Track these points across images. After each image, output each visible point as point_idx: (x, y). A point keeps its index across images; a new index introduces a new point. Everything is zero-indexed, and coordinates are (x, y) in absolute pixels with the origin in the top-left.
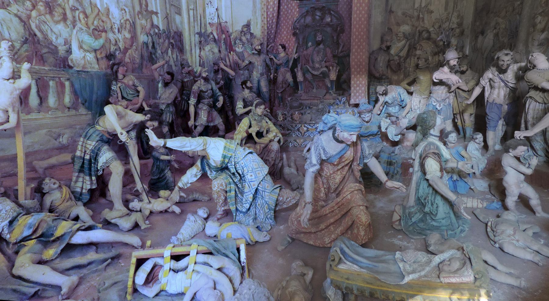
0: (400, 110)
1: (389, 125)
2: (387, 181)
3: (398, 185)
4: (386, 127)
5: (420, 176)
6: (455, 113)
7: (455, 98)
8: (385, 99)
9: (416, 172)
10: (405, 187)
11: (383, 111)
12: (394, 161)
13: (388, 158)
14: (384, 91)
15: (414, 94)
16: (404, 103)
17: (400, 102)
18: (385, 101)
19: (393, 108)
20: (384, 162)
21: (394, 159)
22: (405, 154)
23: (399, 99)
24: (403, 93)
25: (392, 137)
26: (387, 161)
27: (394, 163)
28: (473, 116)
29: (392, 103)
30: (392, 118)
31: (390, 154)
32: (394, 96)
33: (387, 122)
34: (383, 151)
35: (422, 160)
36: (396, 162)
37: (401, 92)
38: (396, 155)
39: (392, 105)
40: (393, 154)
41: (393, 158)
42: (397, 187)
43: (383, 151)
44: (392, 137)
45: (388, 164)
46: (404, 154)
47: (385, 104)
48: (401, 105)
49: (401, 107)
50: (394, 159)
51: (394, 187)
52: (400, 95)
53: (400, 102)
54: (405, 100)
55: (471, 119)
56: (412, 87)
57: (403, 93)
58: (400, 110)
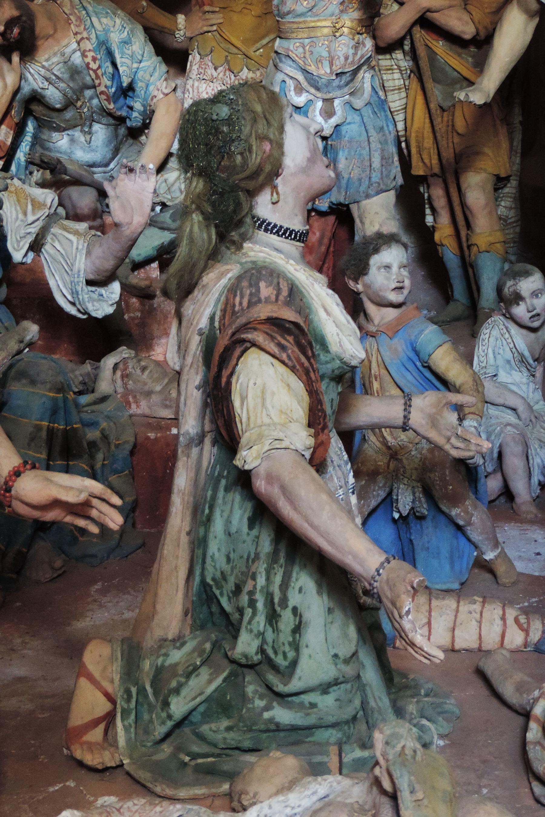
0: (116, 151)
1: (52, 218)
2: (17, 473)
3: (81, 491)
4: (34, 229)
5: (214, 467)
6: (418, 170)
7: (415, 85)
8: (22, 77)
9: (188, 446)
10: (116, 500)
11: (21, 155)
12: (93, 434)
13: (54, 412)
14: (10, 24)
15: (194, 59)
16: (138, 106)
17: (115, 98)
18: (26, 89)
19: (77, 133)
20: (33, 438)
21: (93, 424)
22: (155, 398)
23: (106, 81)
24: (126, 42)
25: (75, 293)
26: (51, 432)
27: (92, 445)
28: (510, 189)
29: (69, 104)
30: (74, 192)
31: (61, 389)
32: (77, 59)
33: (37, 205)
34: (22, 375)
35: (214, 369)
36: (105, 437)
37: (115, 38)
38: (104, 399)
39: (69, 114)
40: (84, 400)
41: (86, 417)
42: (71, 498)
43: (22, 375)
44: (75, 293)
45: (57, 448)
46: (149, 394)
47: (28, 113)
48: (121, 120)
49: (122, 131)
50: (93, 424)
51: (56, 503)
52: (110, 54)
53: (115, 98)
54: (139, 86)
55: (501, 211)
56: (181, 18)
57: (126, 42)
58: (116, 151)
